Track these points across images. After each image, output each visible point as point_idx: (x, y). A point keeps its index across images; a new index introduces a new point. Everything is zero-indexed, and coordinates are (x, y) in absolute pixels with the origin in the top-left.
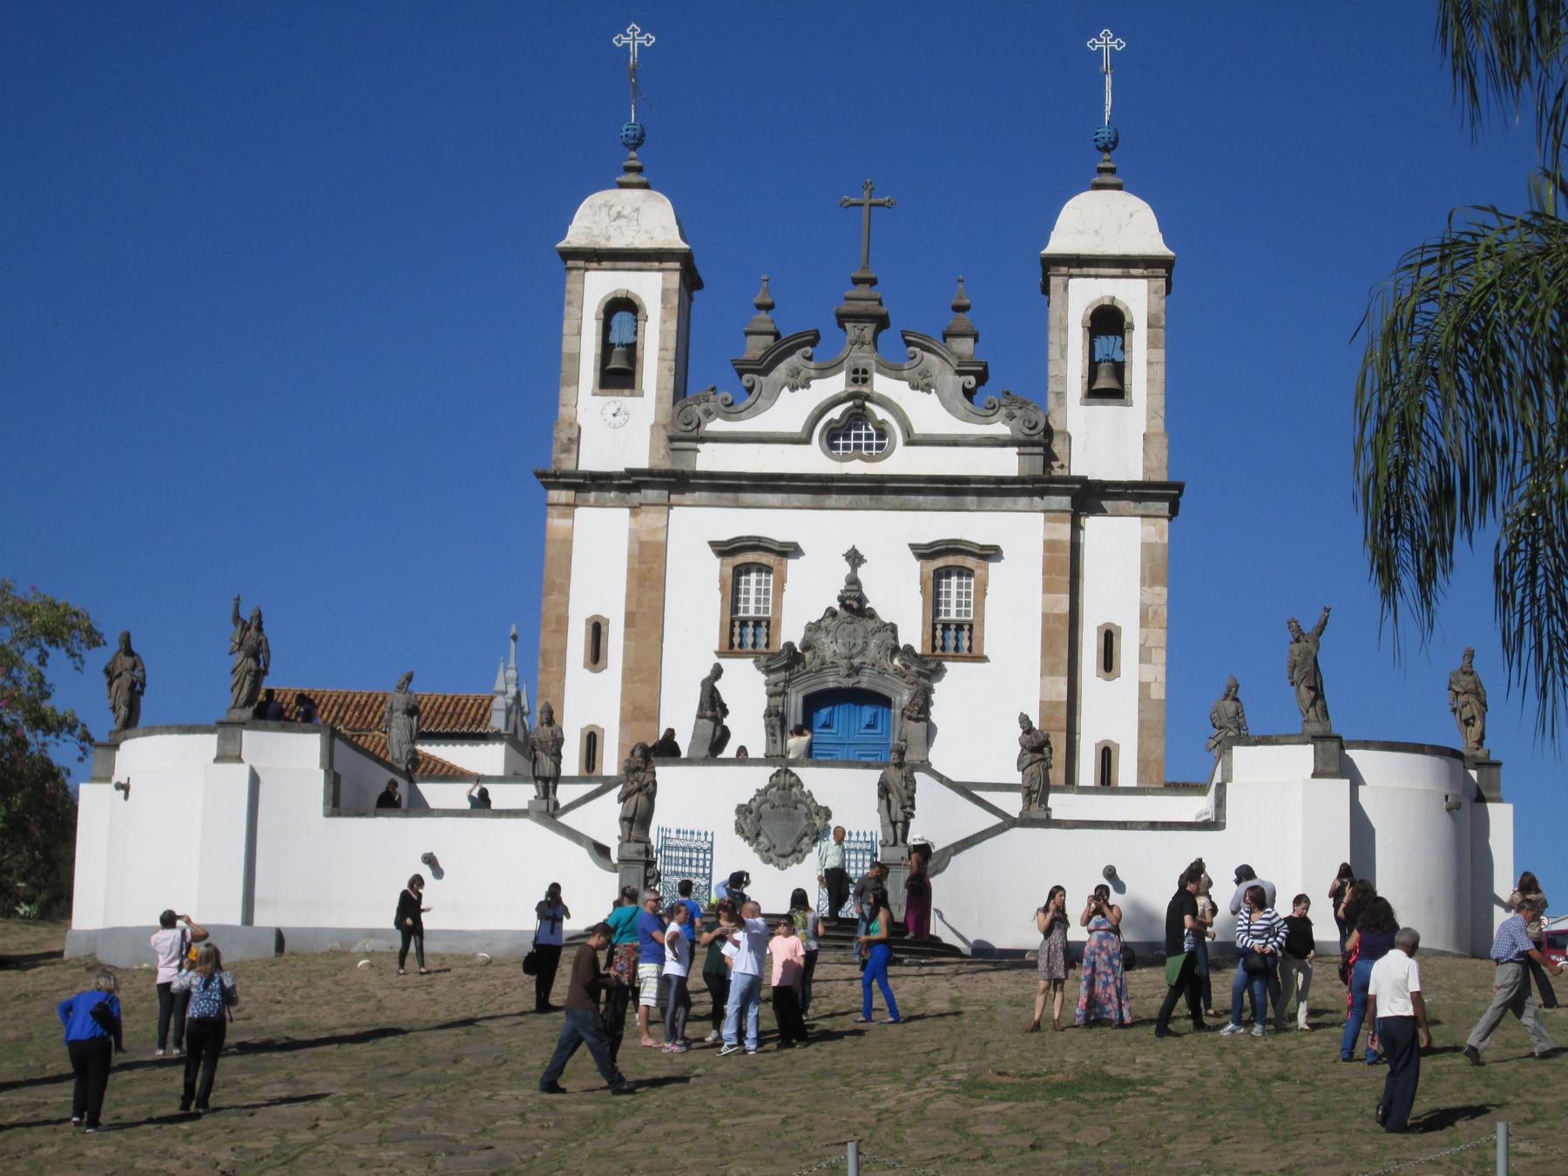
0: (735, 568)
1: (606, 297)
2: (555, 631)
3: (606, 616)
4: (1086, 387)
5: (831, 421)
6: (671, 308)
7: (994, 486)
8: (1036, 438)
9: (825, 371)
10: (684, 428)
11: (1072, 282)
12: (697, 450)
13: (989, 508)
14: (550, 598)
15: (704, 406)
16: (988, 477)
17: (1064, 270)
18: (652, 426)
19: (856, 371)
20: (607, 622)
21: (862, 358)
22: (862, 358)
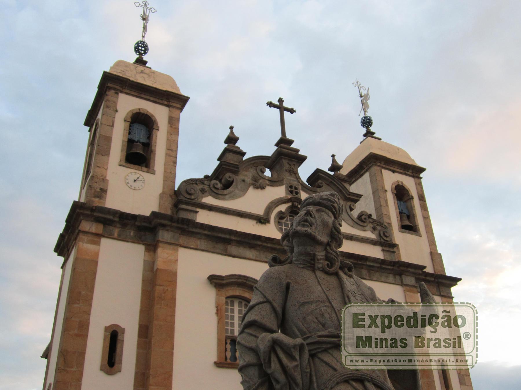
0: (227, 298)
1: (133, 110)
2: (77, 335)
3: (122, 325)
4: (400, 223)
5: (281, 212)
6: (175, 128)
7: (378, 265)
8: (390, 242)
9: (273, 182)
10: (188, 196)
11: (384, 171)
12: (197, 212)
13: (375, 279)
14: (75, 305)
15: (200, 187)
16: (378, 259)
17: (379, 164)
18: (160, 194)
19: (291, 187)
20: (123, 331)
21: (294, 181)
22: (294, 181)
